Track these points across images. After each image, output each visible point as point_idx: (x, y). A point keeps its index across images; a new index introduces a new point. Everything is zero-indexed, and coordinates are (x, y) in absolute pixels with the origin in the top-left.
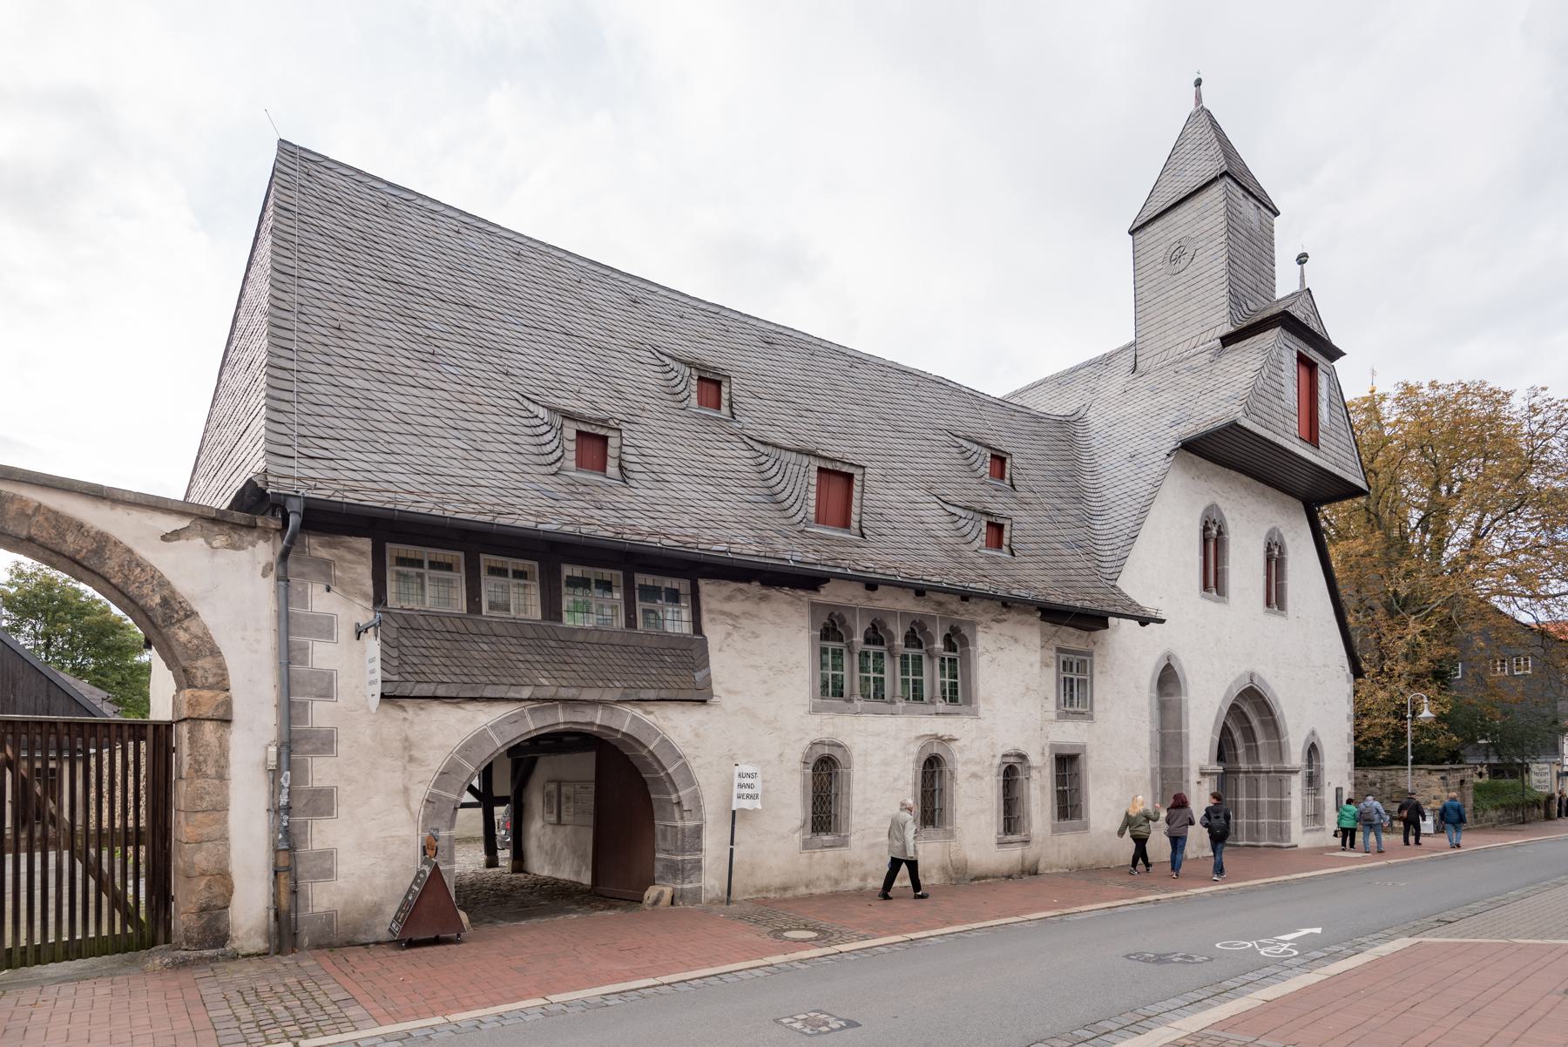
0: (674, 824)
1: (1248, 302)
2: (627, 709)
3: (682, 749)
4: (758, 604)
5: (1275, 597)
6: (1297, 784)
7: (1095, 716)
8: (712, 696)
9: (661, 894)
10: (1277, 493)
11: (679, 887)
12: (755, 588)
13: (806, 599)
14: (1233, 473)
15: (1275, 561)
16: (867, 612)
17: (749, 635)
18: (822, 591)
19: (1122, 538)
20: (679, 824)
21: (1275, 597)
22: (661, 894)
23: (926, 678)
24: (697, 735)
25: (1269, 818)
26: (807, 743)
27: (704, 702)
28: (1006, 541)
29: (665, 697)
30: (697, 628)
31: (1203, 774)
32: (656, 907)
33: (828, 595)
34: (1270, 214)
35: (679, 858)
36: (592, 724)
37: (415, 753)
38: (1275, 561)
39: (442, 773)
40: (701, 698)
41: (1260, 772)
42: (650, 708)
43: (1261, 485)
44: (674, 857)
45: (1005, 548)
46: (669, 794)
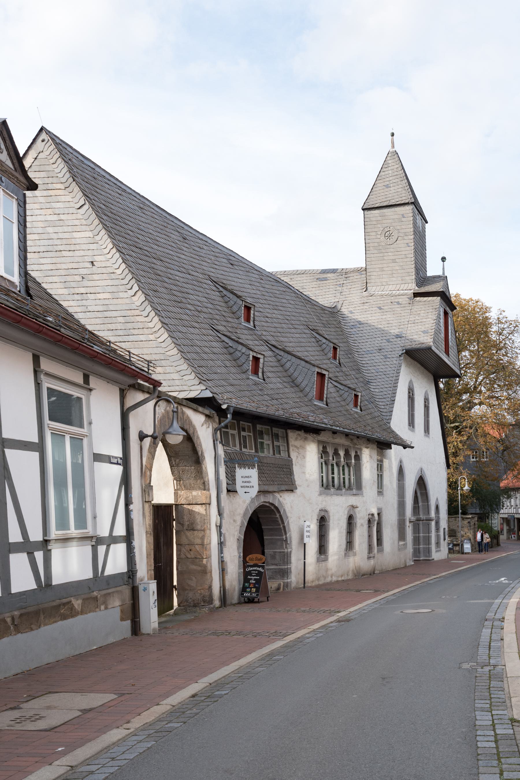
0: (282, 551)
1: (420, 272)
2: (277, 495)
3: (289, 515)
4: (304, 441)
6: (433, 523)
9: (279, 585)
10: (427, 372)
11: (286, 581)
12: (302, 433)
13: (316, 438)
14: (416, 363)
16: (333, 444)
17: (302, 457)
18: (321, 435)
19: (387, 399)
20: (286, 550)
22: (279, 585)
23: (336, 476)
24: (291, 507)
25: (423, 545)
27: (292, 491)
28: (359, 403)
29: (287, 489)
30: (289, 456)
32: (277, 591)
33: (323, 437)
34: (424, 222)
35: (286, 567)
36: (269, 503)
37: (235, 518)
39: (241, 527)
40: (291, 488)
41: (420, 520)
42: (281, 494)
43: (423, 368)
44: (283, 567)
45: (359, 407)
46: (282, 536)
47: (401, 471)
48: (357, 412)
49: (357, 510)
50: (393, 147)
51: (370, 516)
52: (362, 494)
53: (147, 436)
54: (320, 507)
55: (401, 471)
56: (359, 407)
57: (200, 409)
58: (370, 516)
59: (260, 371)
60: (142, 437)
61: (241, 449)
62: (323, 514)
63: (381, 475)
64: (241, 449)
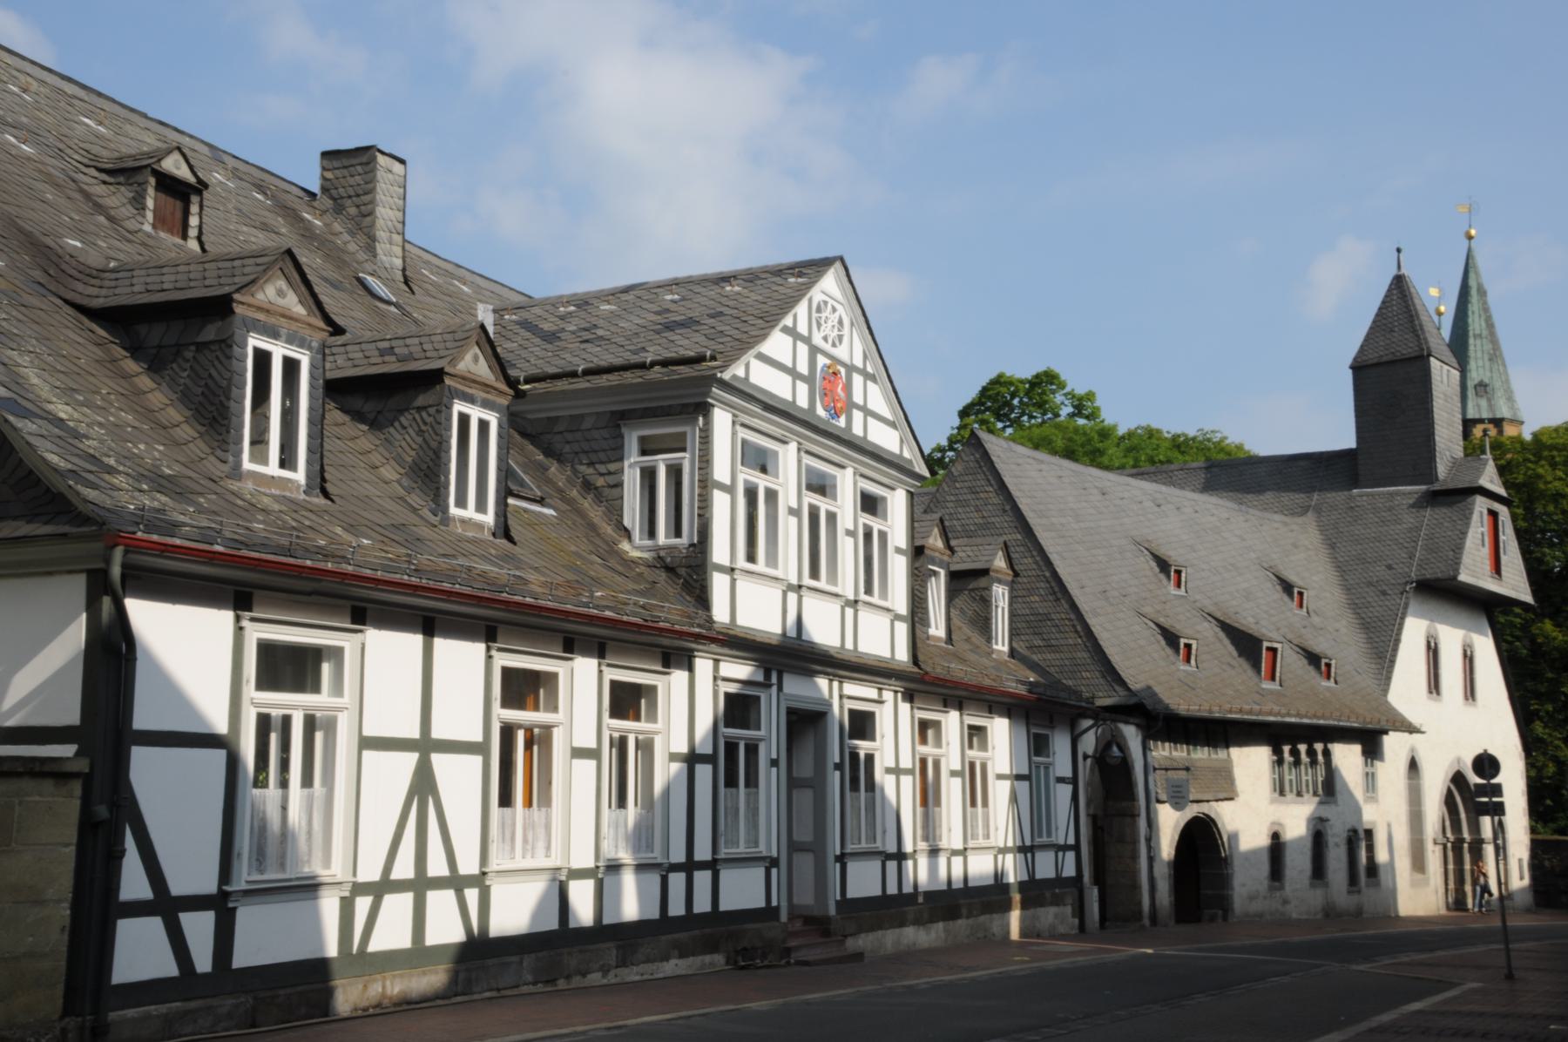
2: (1213, 804)
5: (1470, 692)
7: (1380, 798)
8: (1237, 795)
15: (1469, 659)
21: (1470, 692)
26: (1268, 824)
31: (1435, 843)
38: (1469, 659)
45: (1332, 680)
47: (1413, 765)
48: (1328, 689)
49: (1327, 824)
50: (1399, 267)
51: (1351, 834)
52: (1335, 802)
53: (1089, 757)
54: (1272, 819)
55: (1413, 765)
56: (1332, 680)
57: (1132, 720)
58: (1351, 834)
59: (1193, 658)
60: (1086, 757)
61: (1171, 753)
62: (1276, 828)
63: (1373, 774)
64: (1171, 753)
